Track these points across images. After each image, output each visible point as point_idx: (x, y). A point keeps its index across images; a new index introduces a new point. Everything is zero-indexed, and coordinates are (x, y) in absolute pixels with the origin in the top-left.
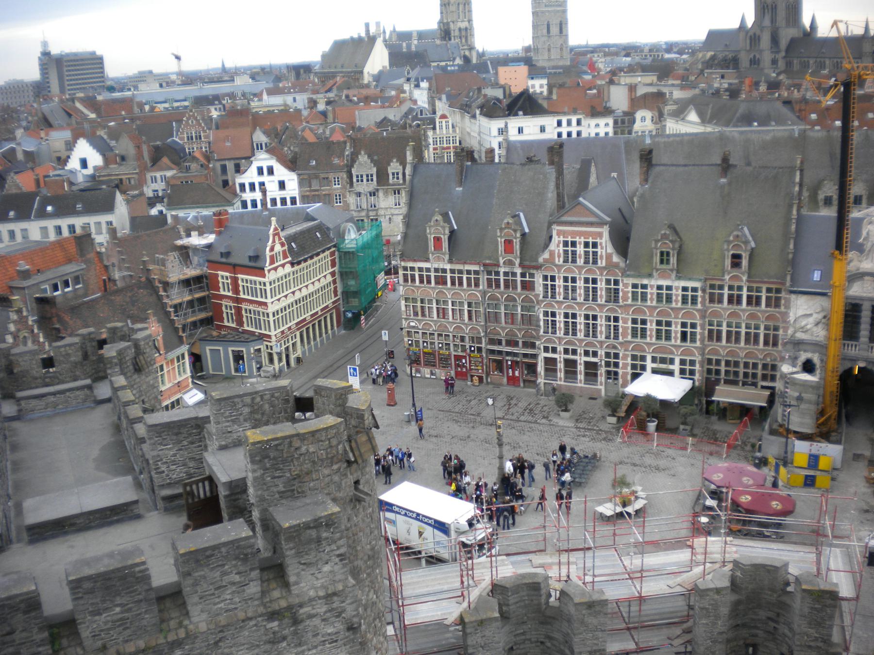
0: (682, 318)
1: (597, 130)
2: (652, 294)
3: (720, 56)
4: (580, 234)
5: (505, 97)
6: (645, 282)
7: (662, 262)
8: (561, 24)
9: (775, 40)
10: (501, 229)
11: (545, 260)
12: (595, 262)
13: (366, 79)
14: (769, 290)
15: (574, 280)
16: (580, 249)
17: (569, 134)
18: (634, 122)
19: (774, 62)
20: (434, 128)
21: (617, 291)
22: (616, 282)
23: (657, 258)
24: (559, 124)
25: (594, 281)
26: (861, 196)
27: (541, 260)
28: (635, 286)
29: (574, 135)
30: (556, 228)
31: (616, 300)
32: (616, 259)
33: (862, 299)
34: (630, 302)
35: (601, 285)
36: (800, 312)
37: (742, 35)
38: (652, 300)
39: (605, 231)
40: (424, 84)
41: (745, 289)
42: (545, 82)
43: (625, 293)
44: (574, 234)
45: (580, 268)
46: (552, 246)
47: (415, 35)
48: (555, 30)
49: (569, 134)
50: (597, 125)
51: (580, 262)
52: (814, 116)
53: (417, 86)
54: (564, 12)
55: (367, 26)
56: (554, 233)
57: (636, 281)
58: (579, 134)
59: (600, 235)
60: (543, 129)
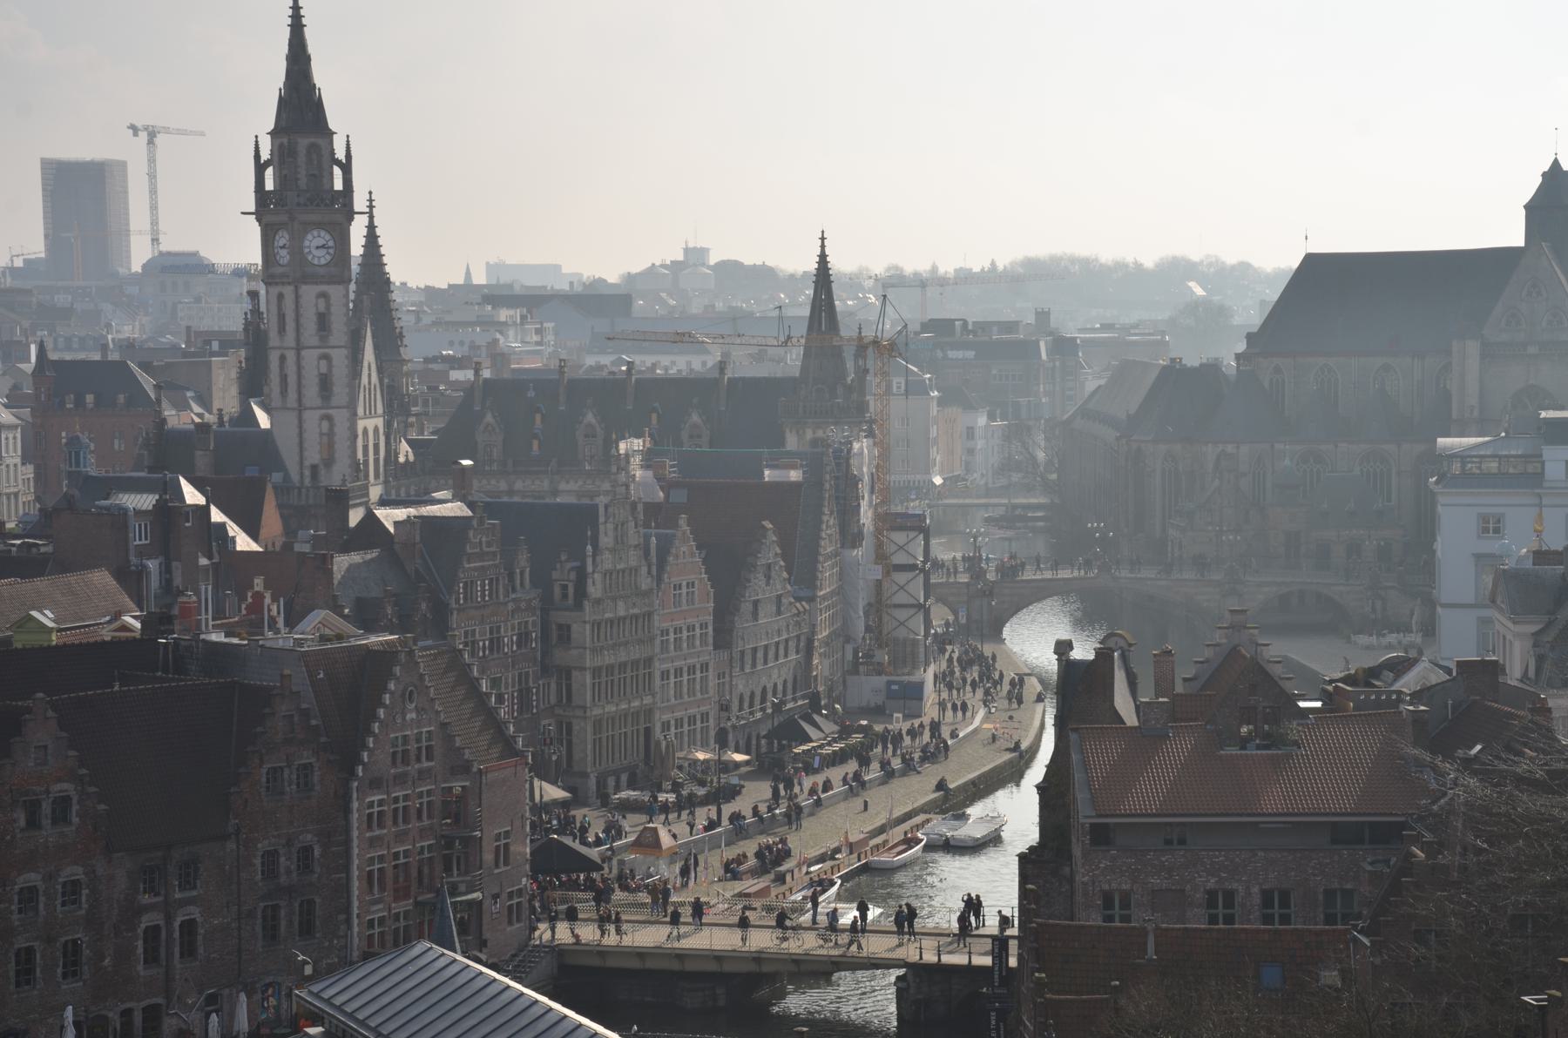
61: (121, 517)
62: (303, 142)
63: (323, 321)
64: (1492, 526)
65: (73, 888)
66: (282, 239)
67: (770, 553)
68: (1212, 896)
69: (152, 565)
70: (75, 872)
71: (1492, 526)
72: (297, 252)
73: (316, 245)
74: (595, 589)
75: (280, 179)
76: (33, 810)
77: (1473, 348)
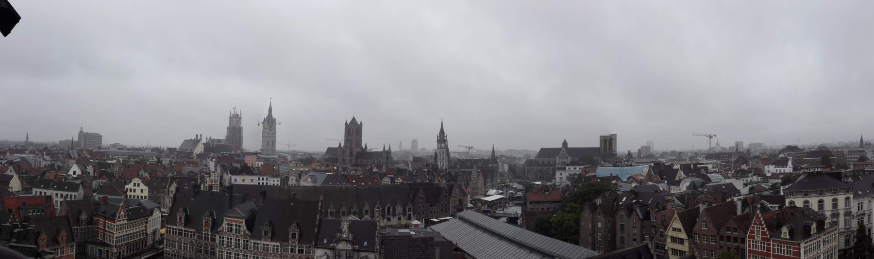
0: (273, 257)
1: (274, 183)
2: (261, 247)
3: (331, 157)
4: (234, 221)
5: (241, 167)
6: (258, 242)
7: (265, 235)
8: (273, 142)
9: (351, 153)
10: (205, 216)
11: (220, 231)
12: (239, 233)
13: (194, 155)
14: (306, 248)
15: (231, 239)
16: (234, 227)
17: (263, 183)
18: (289, 180)
19: (351, 160)
20: (210, 177)
21: (247, 245)
22: (247, 241)
23: (263, 233)
24: (259, 179)
25: (239, 240)
26: (368, 211)
27: (219, 230)
28: (254, 243)
29: (265, 184)
30: (225, 218)
31: (247, 249)
32: (247, 232)
33: (342, 250)
34: (252, 249)
35: (241, 242)
36: (319, 255)
37: (339, 150)
38: (261, 249)
39: (244, 221)
40: (214, 160)
41: (297, 247)
42: (262, 163)
43: (251, 246)
44: (232, 221)
45: (233, 235)
46: (223, 225)
47: (216, 141)
48: (270, 143)
49: (263, 183)
50: (274, 181)
51: (234, 232)
52: (354, 181)
53: (211, 160)
54: (275, 137)
55: (197, 135)
56: (224, 220)
57: (255, 242)
58: (267, 183)
59: (242, 222)
60: (252, 180)
61: (424, 171)
62: (442, 135)
63: (443, 153)
64: (561, 174)
65: (424, 206)
66: (440, 144)
67: (489, 176)
68: (542, 209)
69: (427, 176)
70: (424, 205)
71: (561, 174)
72: (441, 146)
73: (443, 145)
74: (472, 179)
75: (440, 139)
76: (420, 198)
77: (558, 157)
